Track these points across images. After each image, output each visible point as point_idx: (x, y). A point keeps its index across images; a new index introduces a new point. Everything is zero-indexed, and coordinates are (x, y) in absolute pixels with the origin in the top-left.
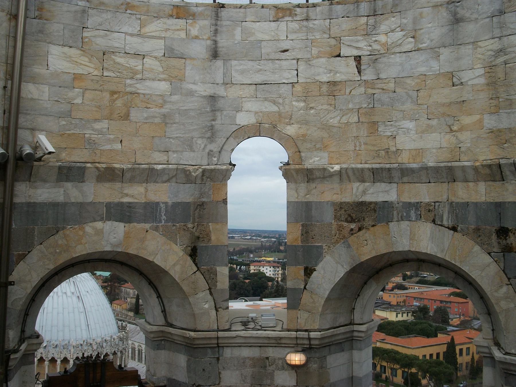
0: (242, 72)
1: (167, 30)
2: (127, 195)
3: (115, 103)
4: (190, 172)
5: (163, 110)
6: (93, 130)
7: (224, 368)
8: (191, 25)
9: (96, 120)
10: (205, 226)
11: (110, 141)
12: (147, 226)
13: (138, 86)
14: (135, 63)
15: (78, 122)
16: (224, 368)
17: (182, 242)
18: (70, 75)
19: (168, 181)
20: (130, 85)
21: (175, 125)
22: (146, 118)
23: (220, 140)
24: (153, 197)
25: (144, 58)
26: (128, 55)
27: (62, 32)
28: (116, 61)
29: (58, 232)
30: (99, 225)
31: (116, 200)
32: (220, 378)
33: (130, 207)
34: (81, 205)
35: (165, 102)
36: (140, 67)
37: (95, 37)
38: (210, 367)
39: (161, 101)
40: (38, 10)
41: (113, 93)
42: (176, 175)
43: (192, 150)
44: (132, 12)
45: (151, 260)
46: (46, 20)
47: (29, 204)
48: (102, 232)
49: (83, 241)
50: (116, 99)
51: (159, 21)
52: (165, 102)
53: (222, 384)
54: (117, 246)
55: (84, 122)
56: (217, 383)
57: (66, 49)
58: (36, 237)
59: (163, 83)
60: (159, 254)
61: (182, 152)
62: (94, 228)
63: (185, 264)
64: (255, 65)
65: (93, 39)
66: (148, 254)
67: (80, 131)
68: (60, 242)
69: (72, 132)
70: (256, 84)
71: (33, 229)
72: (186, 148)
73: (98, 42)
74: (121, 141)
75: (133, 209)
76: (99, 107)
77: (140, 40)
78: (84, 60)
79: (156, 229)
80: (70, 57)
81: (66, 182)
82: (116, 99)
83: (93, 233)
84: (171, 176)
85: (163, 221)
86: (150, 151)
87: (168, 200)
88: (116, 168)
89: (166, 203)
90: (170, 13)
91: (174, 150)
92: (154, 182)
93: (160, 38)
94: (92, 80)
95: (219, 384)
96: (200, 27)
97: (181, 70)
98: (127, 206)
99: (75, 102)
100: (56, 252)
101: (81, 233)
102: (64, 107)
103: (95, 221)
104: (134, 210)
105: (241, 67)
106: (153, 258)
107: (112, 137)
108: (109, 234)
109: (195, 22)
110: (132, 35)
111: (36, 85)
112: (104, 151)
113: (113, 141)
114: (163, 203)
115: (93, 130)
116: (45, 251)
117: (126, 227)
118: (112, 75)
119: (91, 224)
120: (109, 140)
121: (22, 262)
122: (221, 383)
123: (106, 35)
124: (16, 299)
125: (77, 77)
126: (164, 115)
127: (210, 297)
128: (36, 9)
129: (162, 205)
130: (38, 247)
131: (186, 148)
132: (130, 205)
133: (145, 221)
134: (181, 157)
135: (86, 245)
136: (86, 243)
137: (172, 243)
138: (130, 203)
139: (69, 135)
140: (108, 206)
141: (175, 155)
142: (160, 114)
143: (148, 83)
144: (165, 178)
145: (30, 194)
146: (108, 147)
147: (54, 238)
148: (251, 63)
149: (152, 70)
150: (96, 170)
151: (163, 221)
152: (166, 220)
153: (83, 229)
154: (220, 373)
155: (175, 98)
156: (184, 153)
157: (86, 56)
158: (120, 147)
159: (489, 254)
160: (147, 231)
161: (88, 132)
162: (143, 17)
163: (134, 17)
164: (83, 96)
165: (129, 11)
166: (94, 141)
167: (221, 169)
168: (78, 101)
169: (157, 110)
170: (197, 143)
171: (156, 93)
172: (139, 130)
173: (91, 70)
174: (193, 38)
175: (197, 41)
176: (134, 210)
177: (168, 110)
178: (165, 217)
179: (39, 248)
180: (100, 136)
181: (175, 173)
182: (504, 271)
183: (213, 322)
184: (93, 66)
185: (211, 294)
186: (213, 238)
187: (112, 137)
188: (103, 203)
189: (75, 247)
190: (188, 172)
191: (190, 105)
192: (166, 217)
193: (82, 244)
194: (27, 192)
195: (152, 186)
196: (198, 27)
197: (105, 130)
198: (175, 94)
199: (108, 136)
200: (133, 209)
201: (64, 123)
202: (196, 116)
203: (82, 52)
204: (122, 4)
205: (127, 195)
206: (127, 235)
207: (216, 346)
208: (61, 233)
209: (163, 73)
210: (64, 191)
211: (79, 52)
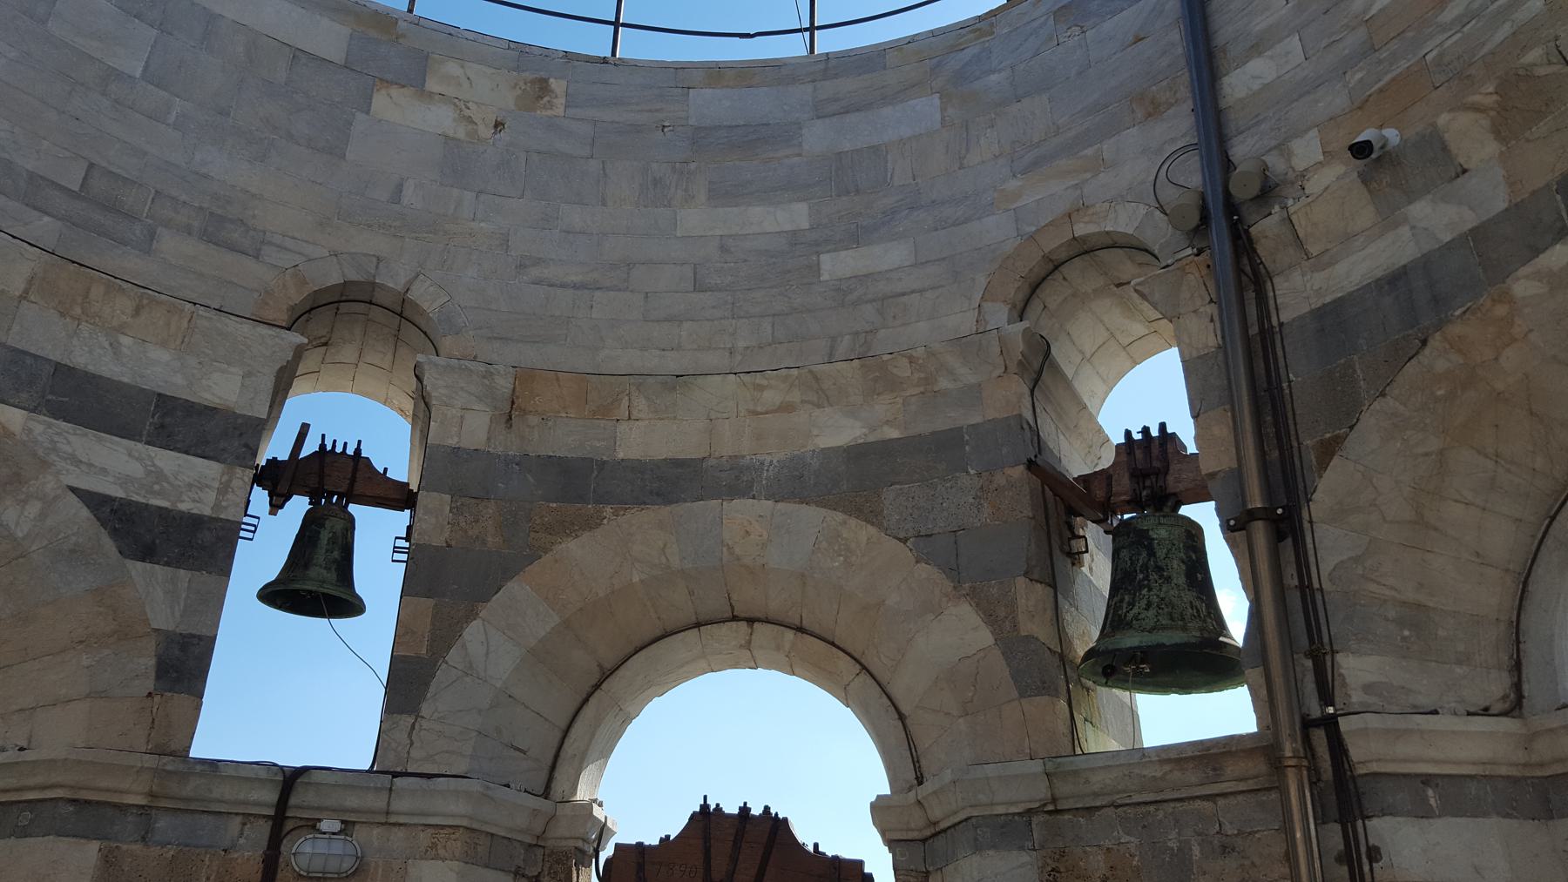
29: (1424, 343)
34: (1478, 235)
47: (1320, 313)
58: (1362, 382)
67: (1409, 61)
68: (1441, 365)
81: (1410, 203)
101: (1501, 310)
103: (1536, 252)
112: (1492, 53)
116: (1401, 408)
121: (1336, 461)
124: (1342, 562)
130: (1376, 405)
136: (1531, 331)
147: (1419, 362)
179: (1378, 408)
188: (1548, 185)
189: (1496, 359)
193: (1516, 340)
194: (1308, 285)
201: (1359, 76)
208: (1436, 341)
210: (1413, 228)
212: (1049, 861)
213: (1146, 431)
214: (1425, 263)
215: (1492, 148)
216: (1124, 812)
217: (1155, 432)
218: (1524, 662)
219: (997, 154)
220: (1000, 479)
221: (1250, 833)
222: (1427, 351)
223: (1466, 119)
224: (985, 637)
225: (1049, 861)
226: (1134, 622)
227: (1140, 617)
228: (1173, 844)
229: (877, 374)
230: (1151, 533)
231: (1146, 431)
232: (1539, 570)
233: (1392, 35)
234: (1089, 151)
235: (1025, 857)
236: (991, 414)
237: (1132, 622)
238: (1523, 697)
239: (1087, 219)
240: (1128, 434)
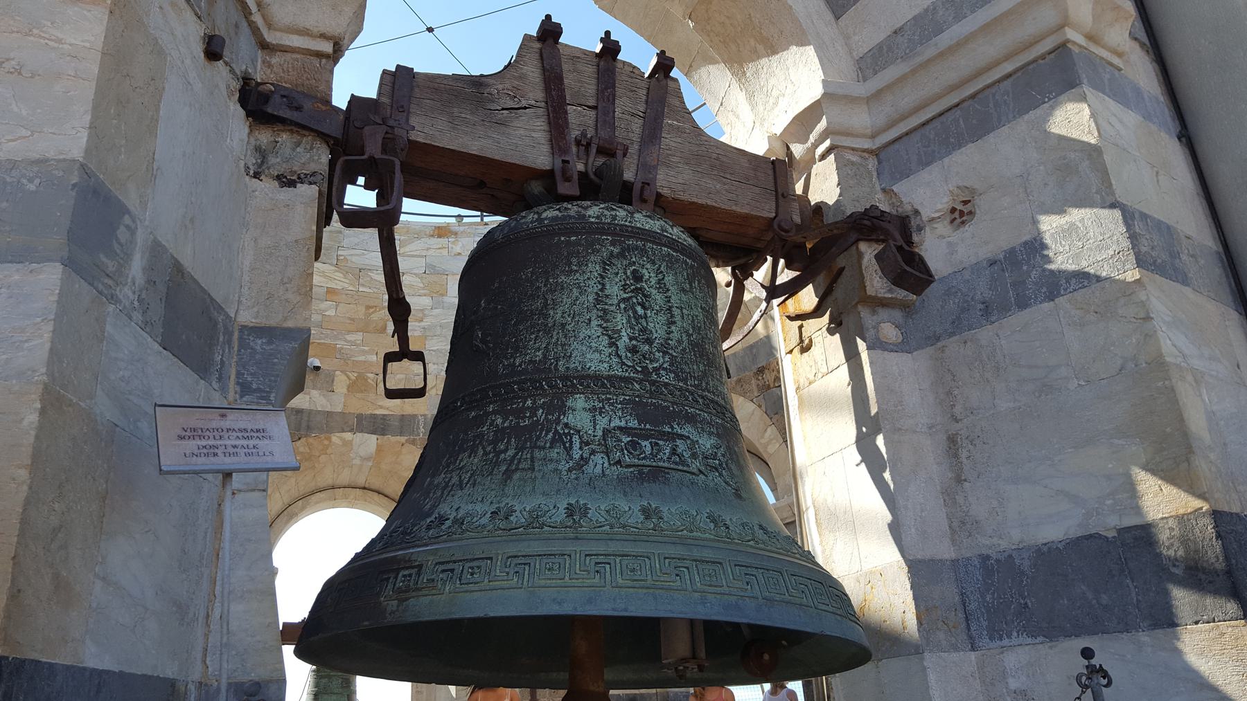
1: (428, 249)
2: (381, 407)
6: (346, 341)
8: (453, 243)
9: (349, 332)
11: (364, 353)
12: (403, 439)
15: (329, 332)
29: (300, 439)
30: (348, 436)
31: (369, 412)
34: (329, 414)
35: (425, 315)
39: (421, 315)
41: (368, 307)
42: (436, 385)
48: (352, 445)
50: (373, 313)
51: (419, 241)
52: (425, 315)
55: (335, 333)
59: (424, 297)
62: (341, 438)
65: (349, 258)
66: (403, 469)
68: (301, 449)
69: (323, 341)
73: (353, 260)
74: (377, 354)
76: (353, 320)
78: (339, 275)
82: (373, 313)
83: (341, 444)
85: (421, 434)
87: (426, 413)
89: (425, 415)
93: (421, 256)
97: (443, 285)
99: (327, 313)
101: (326, 442)
107: (366, 348)
108: (359, 446)
112: (357, 362)
115: (346, 341)
117: (379, 441)
118: (368, 290)
120: (363, 351)
123: (363, 254)
126: (424, 328)
133: (401, 434)
135: (332, 456)
138: (384, 415)
139: (319, 344)
140: (360, 417)
146: (362, 358)
151: (421, 434)
153: (329, 439)
157: (342, 273)
158: (375, 358)
159: (752, 401)
160: (403, 445)
161: (340, 344)
162: (402, 238)
168: (331, 313)
169: (417, 324)
173: (346, 286)
182: (766, 413)
184: (347, 281)
187: (366, 348)
188: (354, 414)
189: (319, 456)
197: (358, 342)
198: (436, 308)
205: (381, 407)
206: (380, 449)
208: (303, 440)
209: (423, 289)
211: (333, 268)
214: (310, 412)
215: (345, 390)
222: (300, 442)
223: (344, 377)
232: (278, 521)
233: (329, 327)
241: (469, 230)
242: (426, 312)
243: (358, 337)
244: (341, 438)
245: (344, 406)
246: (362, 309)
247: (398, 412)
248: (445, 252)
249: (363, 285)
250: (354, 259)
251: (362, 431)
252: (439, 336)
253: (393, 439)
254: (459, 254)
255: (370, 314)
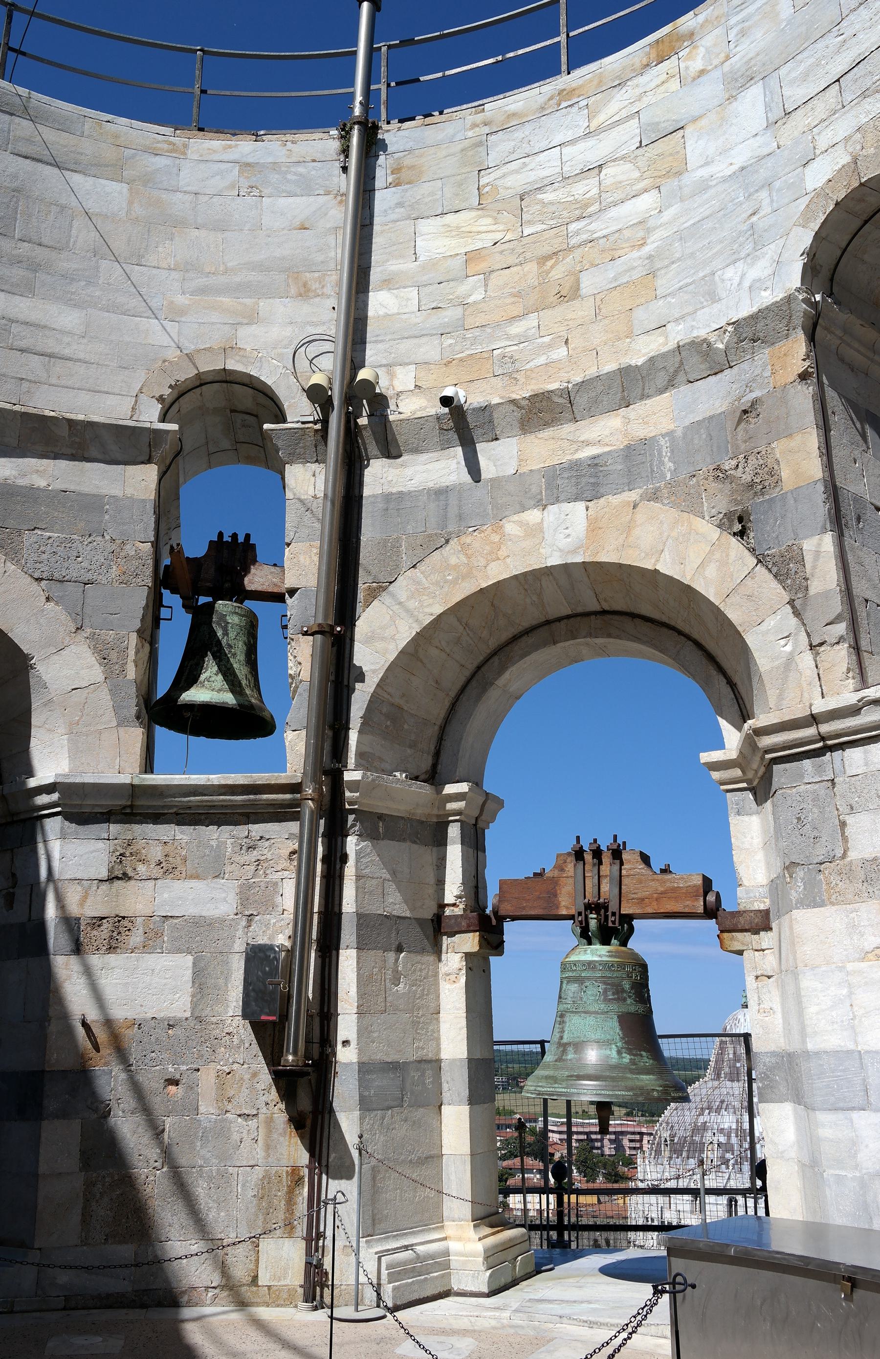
0: (805, 77)
2: (587, 443)
3: (550, 275)
4: (709, 345)
5: (647, 249)
6: (509, 338)
7: (852, 808)
10: (763, 453)
12: (633, 496)
13: (592, 227)
14: (586, 188)
15: (477, 332)
16: (852, 808)
17: (713, 508)
18: (458, 257)
19: (671, 384)
20: (577, 233)
21: (674, 266)
22: (615, 279)
23: (772, 246)
24: (642, 432)
25: (600, 172)
26: (570, 181)
27: (440, 193)
28: (546, 201)
29: (447, 542)
30: (533, 516)
31: (567, 458)
32: (845, 839)
33: (596, 465)
36: (595, 191)
37: (504, 176)
38: (815, 810)
39: (641, 234)
40: (392, 173)
41: (543, 260)
43: (713, 297)
44: (569, 103)
45: (650, 567)
46: (409, 183)
48: (542, 531)
49: (500, 553)
50: (552, 267)
51: (624, 90)
53: (852, 855)
54: (574, 552)
56: (839, 852)
57: (450, 218)
58: (404, 555)
60: (666, 549)
61: (695, 312)
62: (520, 524)
63: (727, 556)
64: (833, 41)
65: (499, 182)
66: (643, 555)
68: (453, 560)
70: (838, 80)
71: (398, 539)
72: (703, 300)
74: (566, 342)
75: (601, 469)
77: (591, 142)
79: (654, 496)
80: (458, 228)
82: (552, 267)
84: (672, 370)
85: (669, 476)
86: (628, 340)
88: (552, 391)
89: (670, 434)
90: (645, 62)
91: (677, 316)
92: (642, 399)
94: (501, 252)
95: (844, 856)
96: (706, 49)
98: (589, 465)
99: (471, 300)
100: (446, 581)
101: (496, 538)
102: (451, 314)
103: (523, 509)
104: (606, 468)
105: (801, 69)
106: (653, 561)
107: (547, 339)
108: (555, 530)
109: (694, 48)
110: (572, 142)
111: (395, 291)
113: (550, 346)
114: (663, 436)
115: (509, 338)
117: (590, 510)
118: (540, 227)
119: (516, 518)
121: (376, 603)
122: (849, 853)
125: (471, 257)
127: (794, 621)
128: (389, 172)
129: (662, 442)
130: (409, 573)
131: (703, 300)
132: (595, 463)
134: (694, 323)
135: (508, 560)
137: (692, 516)
138: (594, 458)
139: (461, 360)
141: (681, 327)
142: (641, 258)
143: (613, 212)
144: (661, 379)
145: (390, 478)
148: (820, 45)
149: (618, 185)
150: (512, 407)
152: (675, 469)
153: (498, 529)
154: (843, 824)
155: (668, 215)
156: (699, 313)
157: (488, 216)
163: (575, 109)
164: (486, 285)
165: (564, 104)
166: (511, 358)
167: (772, 304)
169: (635, 254)
170: (723, 280)
171: (631, 223)
172: (601, 306)
173: (498, 236)
174: (694, 79)
175: (703, 79)
176: (606, 468)
177: (656, 244)
178: (671, 464)
180: (522, 345)
181: (678, 359)
183: (810, 684)
185: (797, 613)
186: (785, 473)
187: (547, 339)
190: (705, 345)
191: (702, 210)
192: (674, 463)
193: (498, 559)
194: (385, 475)
195: (639, 409)
196: (701, 51)
199: (540, 340)
200: (601, 469)
202: (717, 226)
203: (480, 212)
204: (551, 99)
205: (587, 443)
206: (593, 527)
207: (820, 744)
209: (641, 178)
211: (474, 214)
212: (119, 848)
213: (235, 536)
216: (183, 818)
217: (241, 539)
218: (442, 751)
219: (172, 266)
220: (130, 550)
221: (268, 839)
224: (97, 673)
225: (119, 848)
226: (206, 683)
227: (212, 679)
228: (214, 843)
229: (36, 425)
230: (228, 618)
231: (235, 536)
232: (464, 698)
234: (248, 301)
235: (101, 845)
236: (129, 492)
237: (204, 682)
238: (436, 773)
239: (238, 358)
240: (221, 535)
241: (716, 13)
242: (651, 223)
243: (532, 321)
244: (520, 524)
245: (521, 460)
246: (532, 268)
247: (619, 443)
248: (674, 85)
249: (530, 222)
250: (510, 181)
251: (557, 500)
252: (679, 259)
253: (615, 500)
254: (702, 72)
255: (548, 272)
